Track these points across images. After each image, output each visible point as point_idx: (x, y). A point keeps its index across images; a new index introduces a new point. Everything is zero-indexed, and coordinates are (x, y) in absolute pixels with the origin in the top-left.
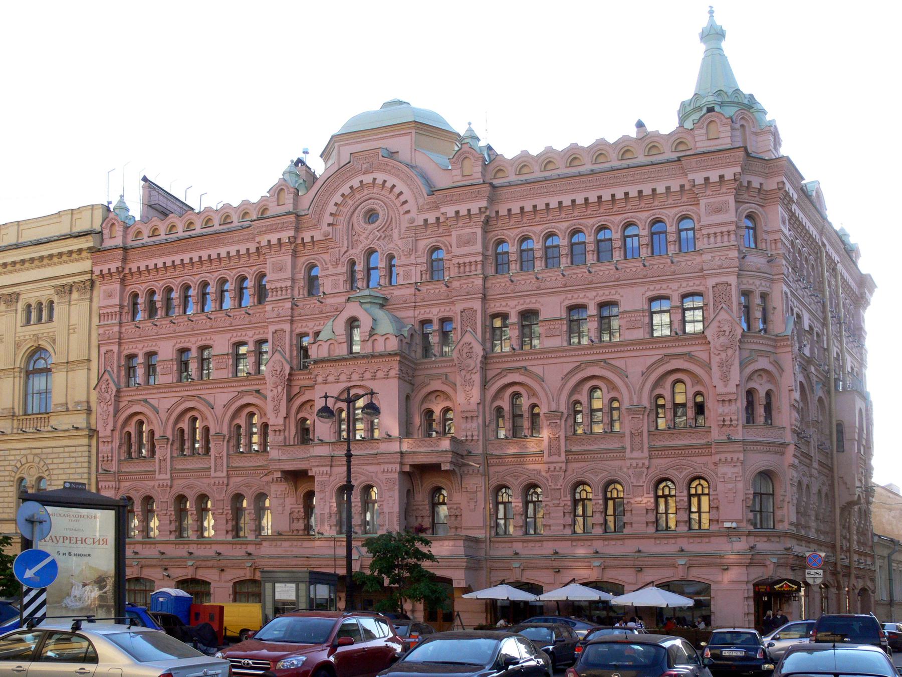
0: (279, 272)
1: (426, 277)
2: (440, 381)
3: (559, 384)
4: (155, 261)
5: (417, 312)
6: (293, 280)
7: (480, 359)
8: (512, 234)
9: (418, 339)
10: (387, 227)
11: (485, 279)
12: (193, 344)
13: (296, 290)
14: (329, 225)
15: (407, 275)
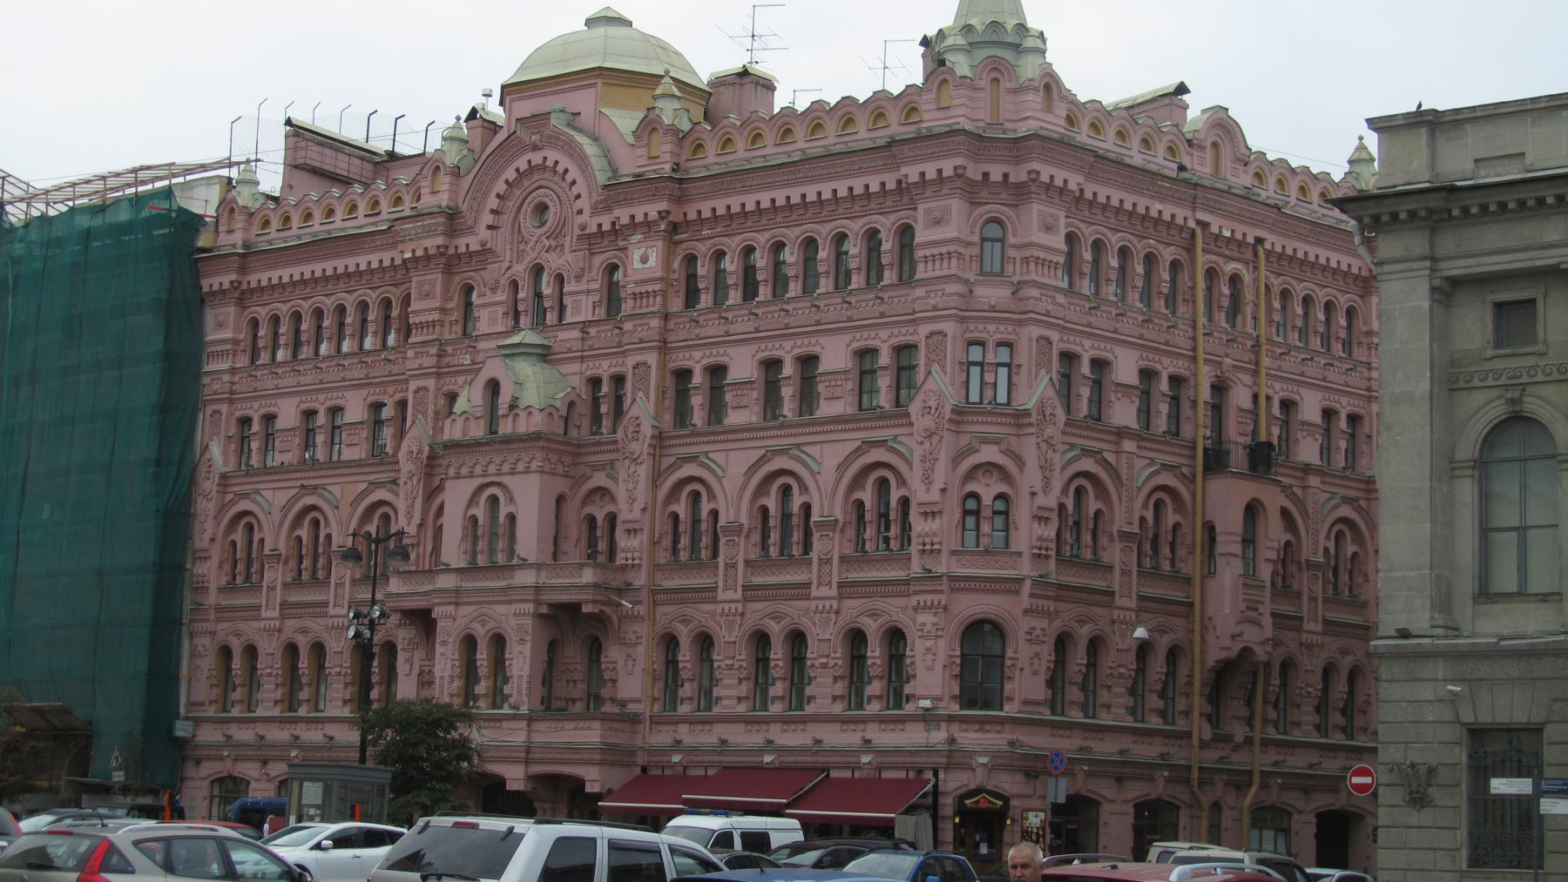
0: (428, 300)
1: (601, 313)
3: (741, 479)
4: (279, 272)
6: (443, 311)
7: (648, 441)
8: (703, 249)
9: (583, 409)
10: (557, 233)
11: (666, 317)
12: (321, 404)
13: (447, 325)
14: (489, 227)
15: (577, 311)
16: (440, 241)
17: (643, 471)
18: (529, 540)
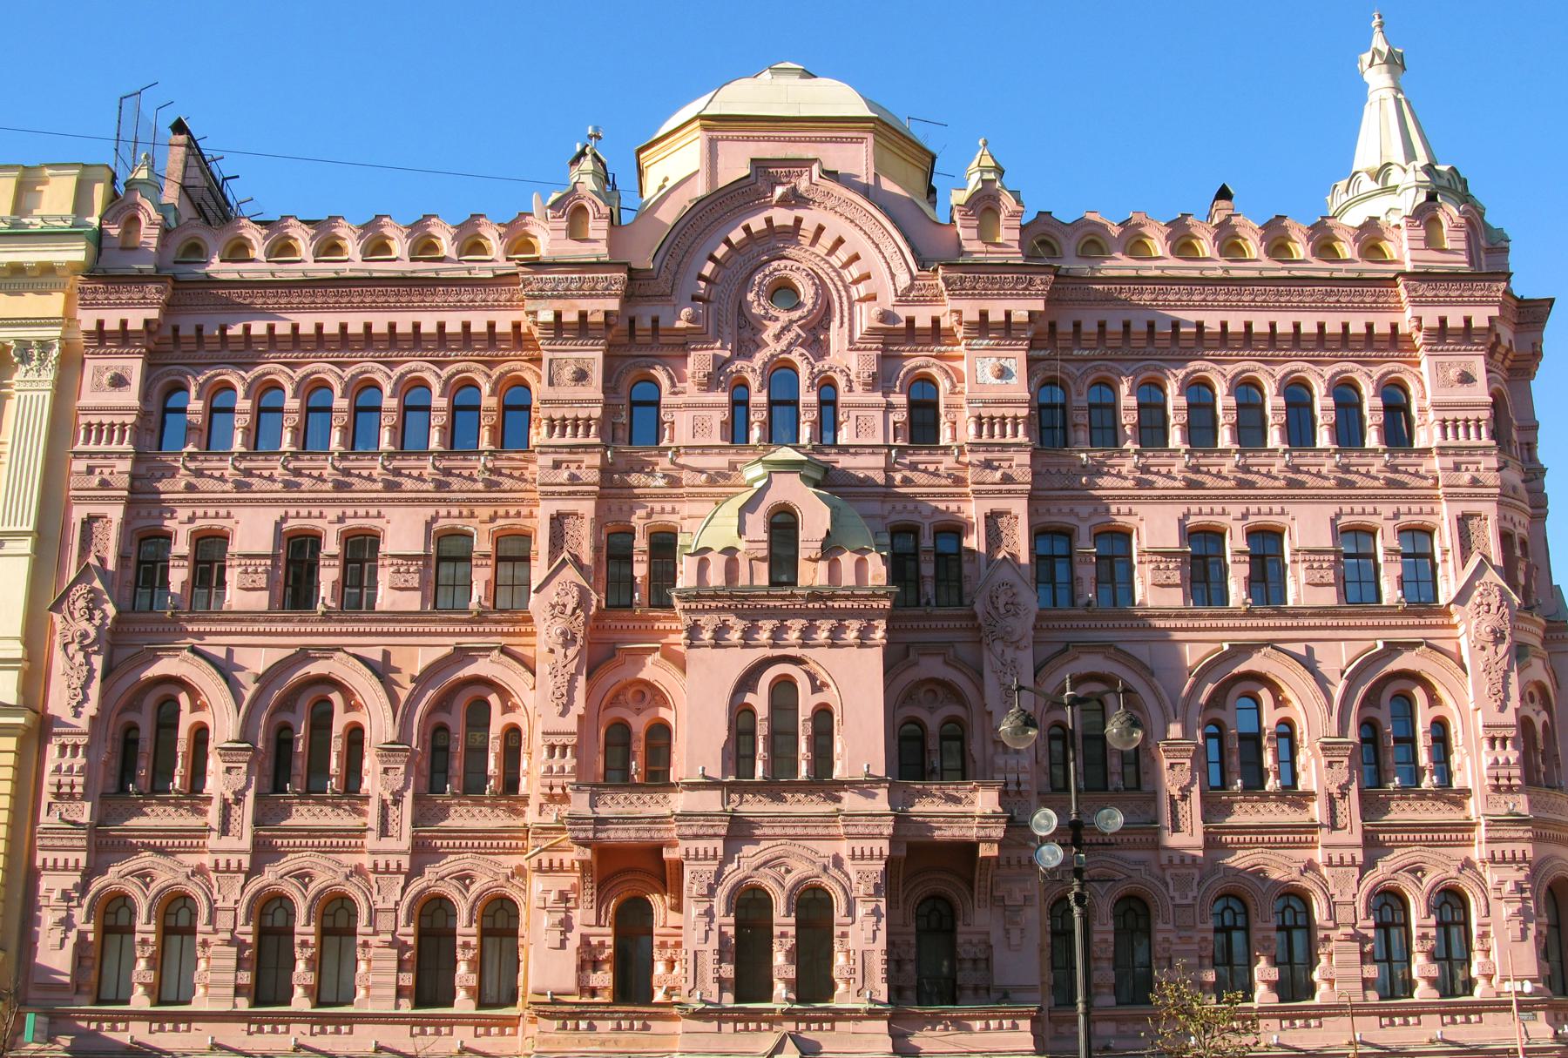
2: (940, 659)
5: (888, 507)
16: (613, 305)
17: (1026, 660)
18: (861, 745)
